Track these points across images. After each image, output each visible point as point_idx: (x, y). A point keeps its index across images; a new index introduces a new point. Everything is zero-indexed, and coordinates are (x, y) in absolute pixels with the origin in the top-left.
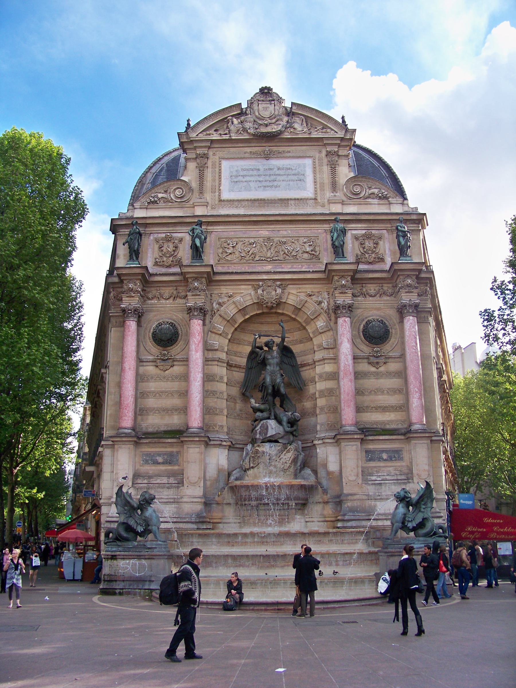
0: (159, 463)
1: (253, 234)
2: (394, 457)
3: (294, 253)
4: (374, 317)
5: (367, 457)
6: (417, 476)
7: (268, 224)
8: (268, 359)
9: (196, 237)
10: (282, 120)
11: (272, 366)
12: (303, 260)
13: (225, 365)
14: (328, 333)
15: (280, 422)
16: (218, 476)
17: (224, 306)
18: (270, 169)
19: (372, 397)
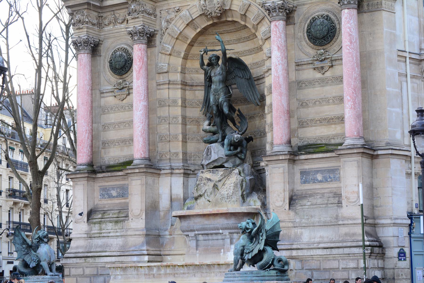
2: (330, 177)
5: (301, 179)
6: (346, 199)
11: (215, 84)
13: (180, 86)
15: (223, 145)
17: (173, 22)
19: (317, 109)
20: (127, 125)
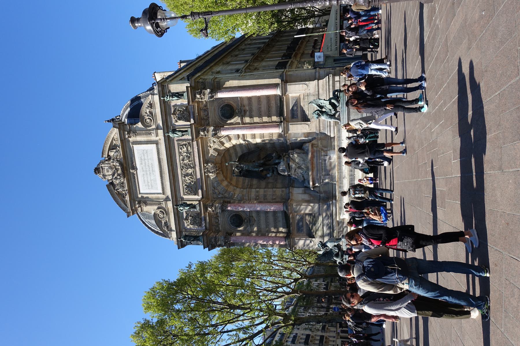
0: (303, 224)
4: (219, 113)
9: (184, 208)
15: (279, 163)
16: (307, 193)
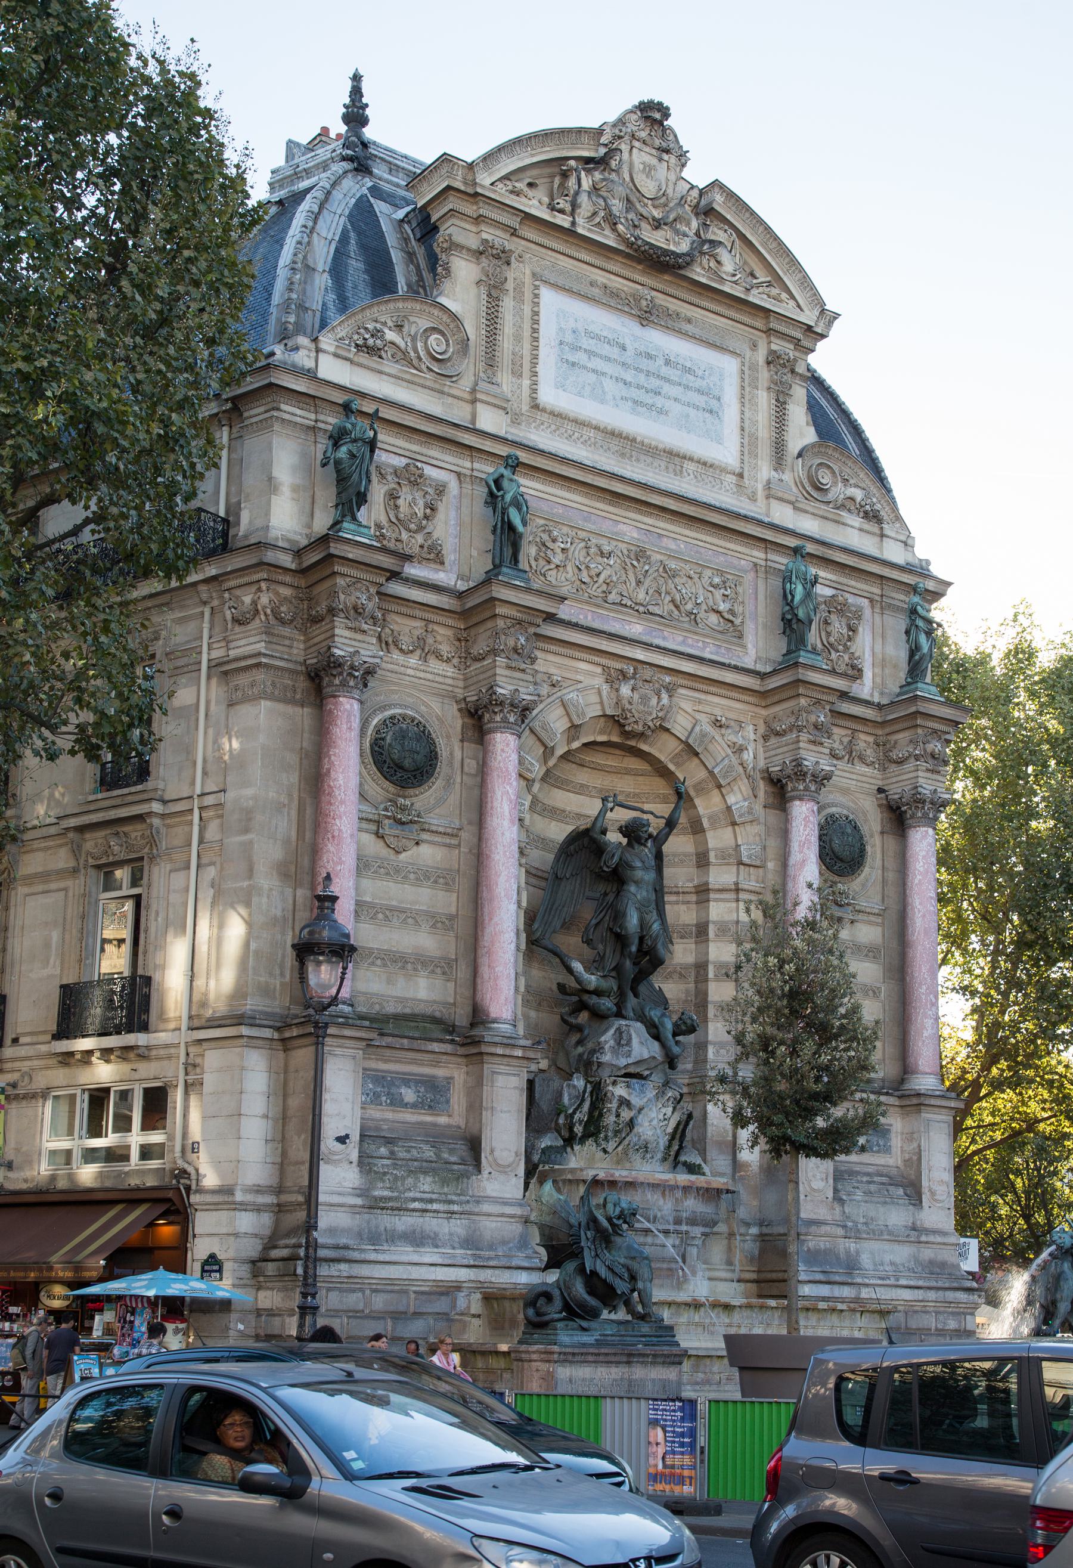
1: (606, 527)
3: (689, 607)
7: (640, 512)
8: (632, 868)
10: (688, 224)
12: (707, 631)
14: (748, 827)
18: (649, 356)
20: (410, 920)
